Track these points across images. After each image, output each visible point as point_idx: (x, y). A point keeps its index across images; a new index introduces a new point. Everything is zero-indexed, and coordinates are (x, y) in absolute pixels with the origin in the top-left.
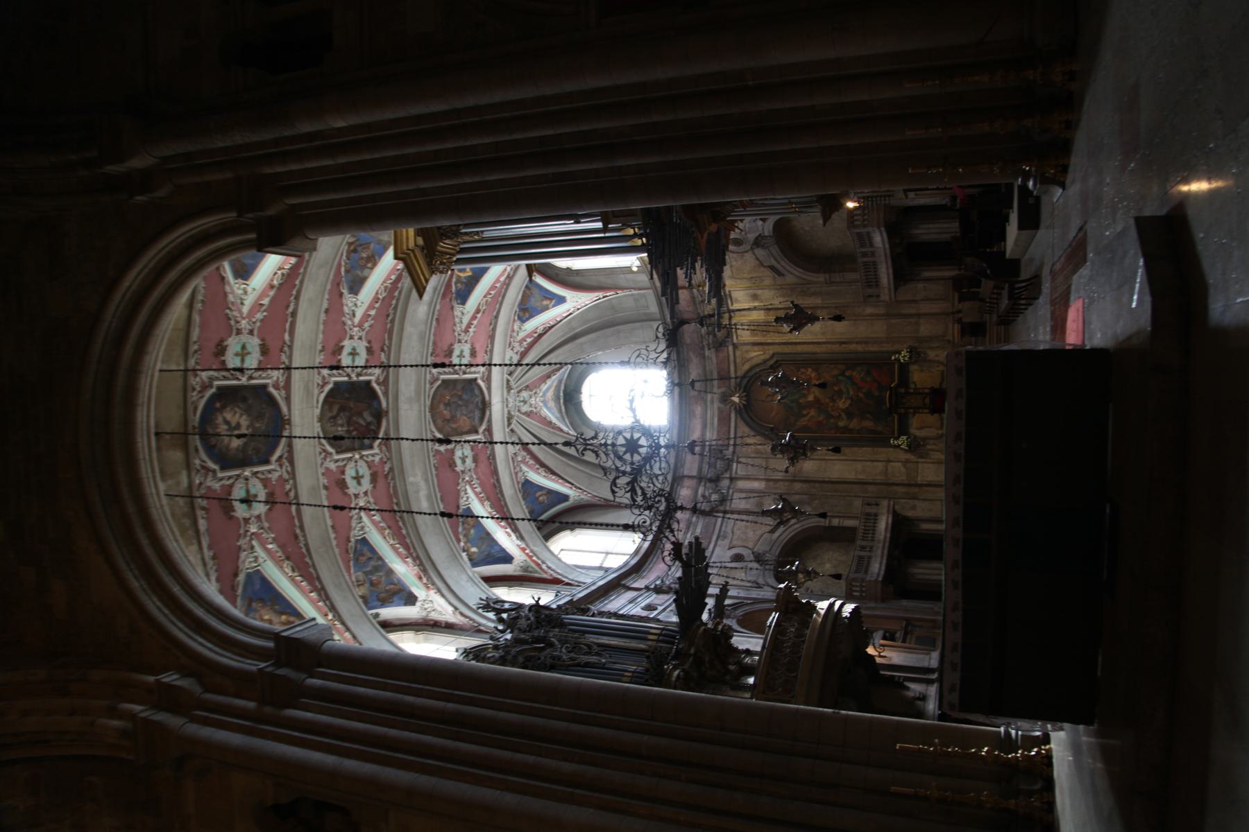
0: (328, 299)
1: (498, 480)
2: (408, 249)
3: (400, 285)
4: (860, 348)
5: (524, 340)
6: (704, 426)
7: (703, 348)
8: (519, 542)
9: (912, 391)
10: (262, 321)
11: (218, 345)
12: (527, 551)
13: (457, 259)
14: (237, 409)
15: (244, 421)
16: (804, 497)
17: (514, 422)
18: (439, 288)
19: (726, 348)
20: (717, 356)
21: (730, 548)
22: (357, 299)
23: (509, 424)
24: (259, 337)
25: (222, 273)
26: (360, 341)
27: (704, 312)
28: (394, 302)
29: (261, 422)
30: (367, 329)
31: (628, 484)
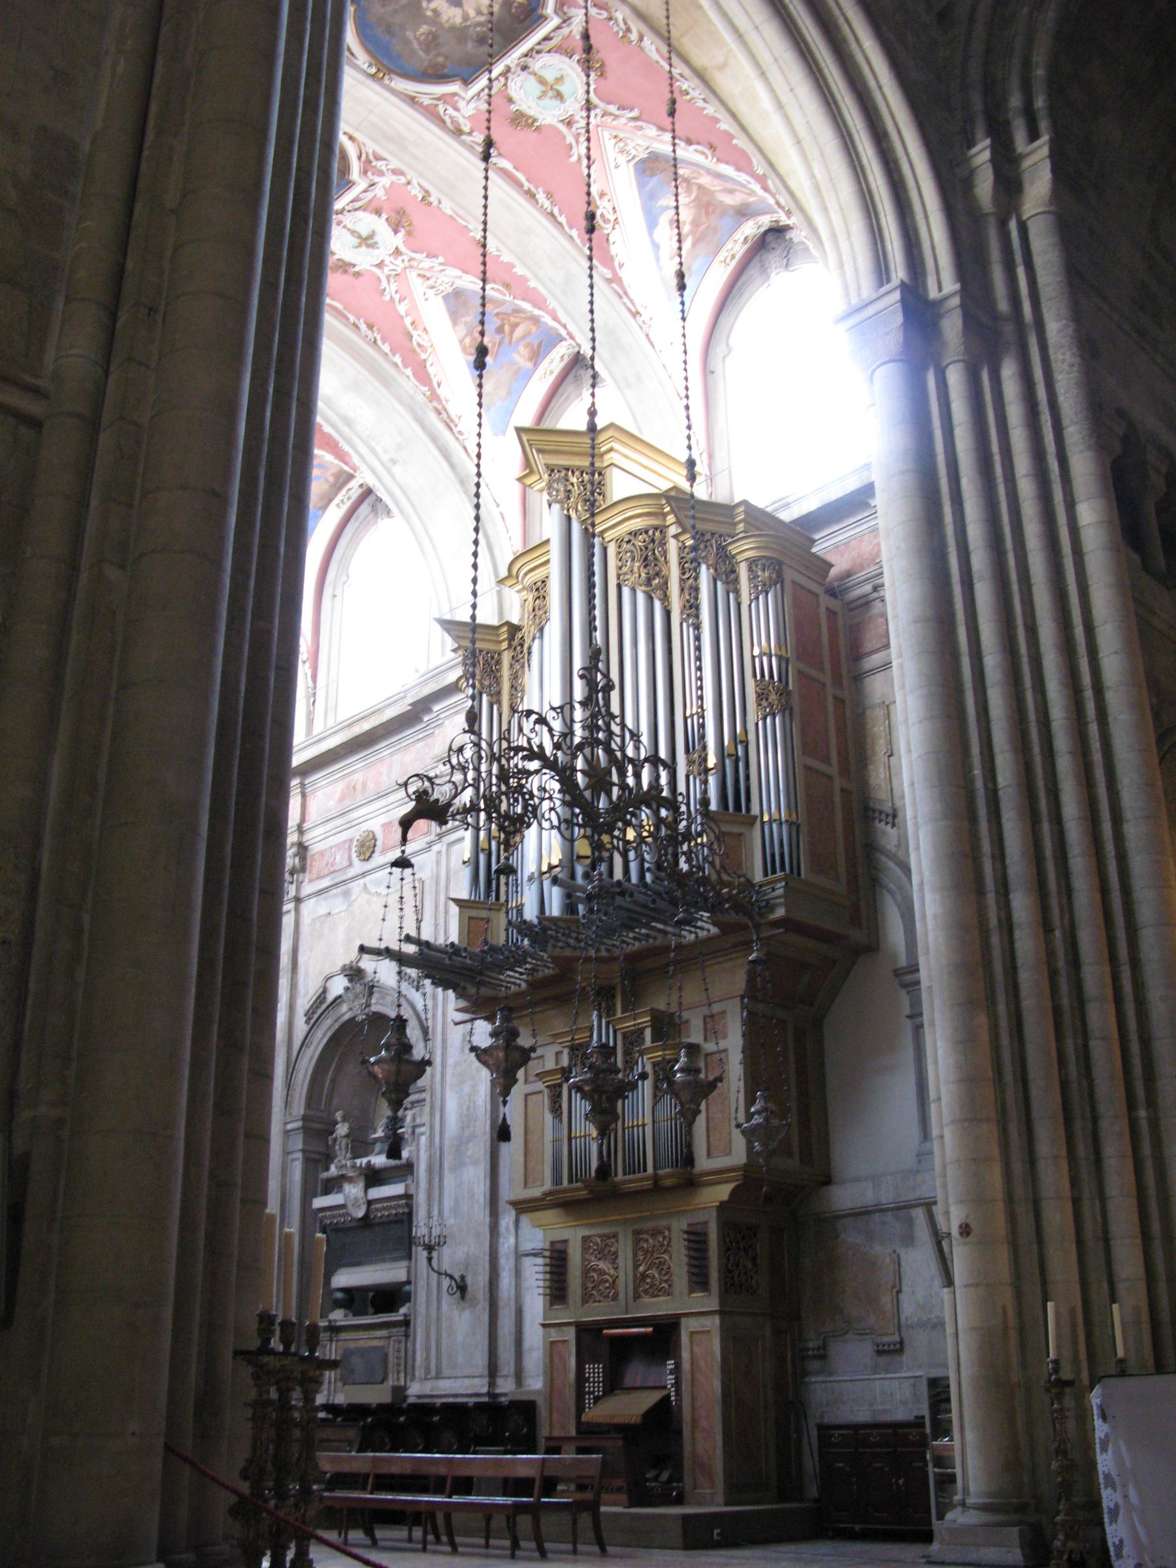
0: (498, 257)
2: (611, 450)
3: (409, 372)
10: (571, 147)
11: (603, 65)
13: (569, 518)
14: (482, 19)
18: (346, 430)
22: (437, 295)
24: (551, 126)
25: (700, 148)
26: (379, 262)
28: (386, 348)
29: (422, 38)
30: (384, 283)
31: (541, 747)
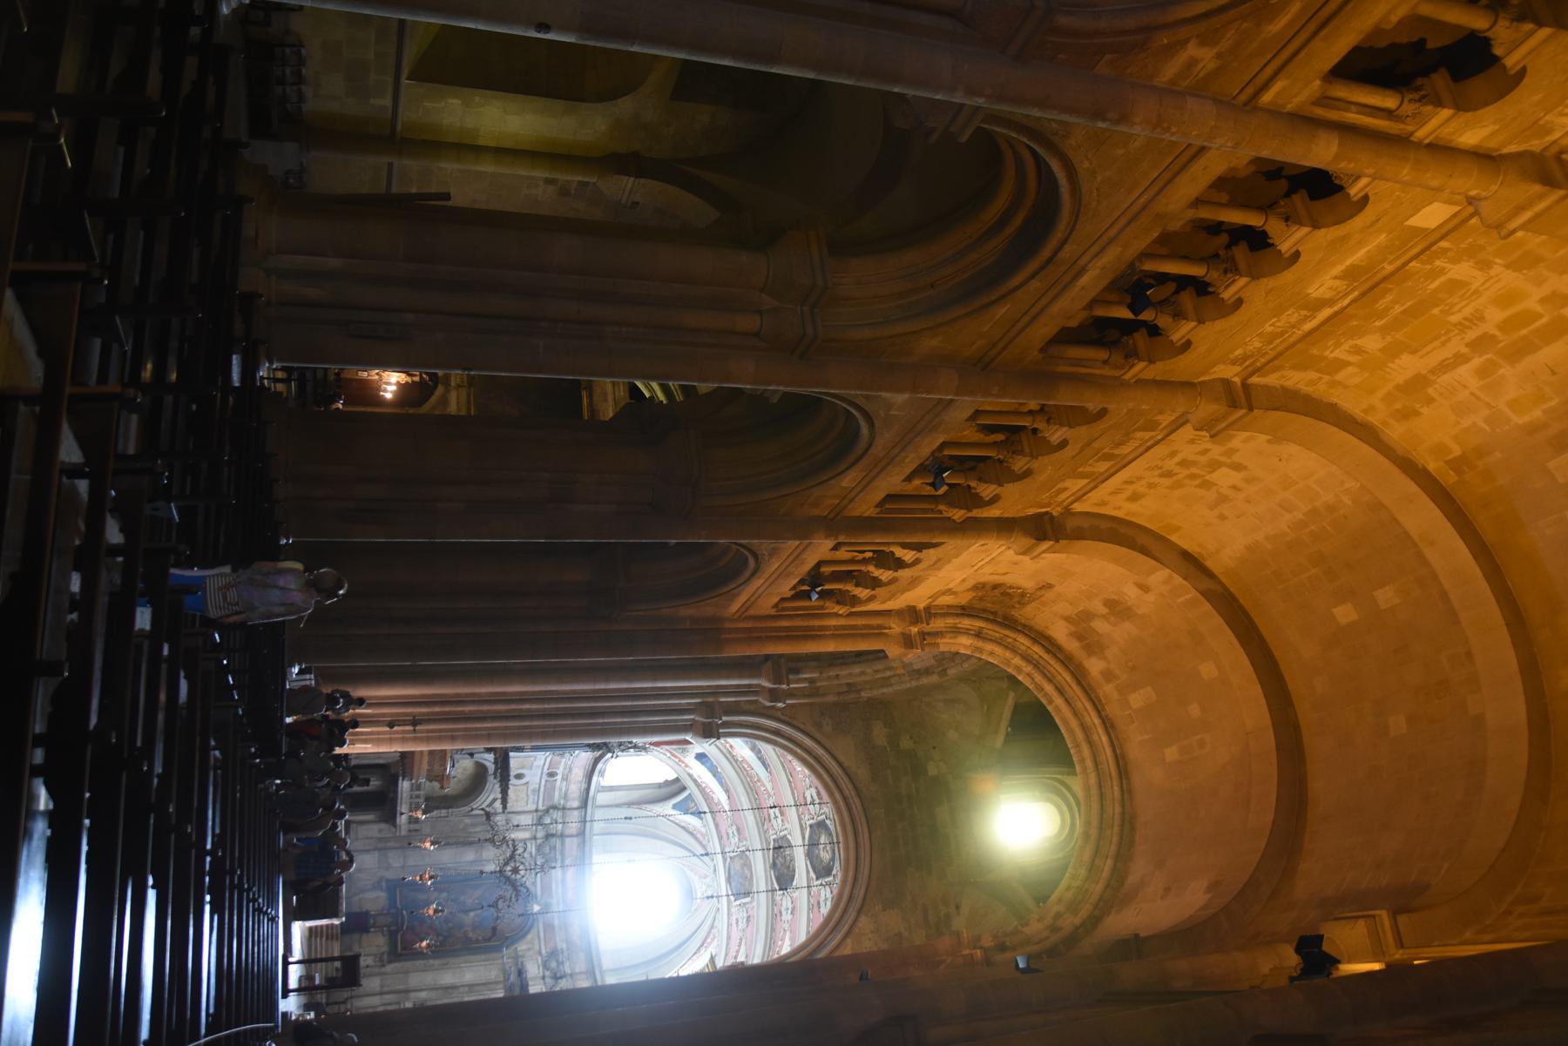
1: (714, 819)
4: (431, 962)
5: (713, 939)
6: (563, 881)
7: (568, 949)
8: (690, 771)
9: (385, 929)
12: (683, 765)
15: (822, 852)
16: (472, 830)
17: (712, 871)
19: (548, 950)
20: (556, 943)
21: (527, 783)
23: (715, 866)
27: (567, 981)
